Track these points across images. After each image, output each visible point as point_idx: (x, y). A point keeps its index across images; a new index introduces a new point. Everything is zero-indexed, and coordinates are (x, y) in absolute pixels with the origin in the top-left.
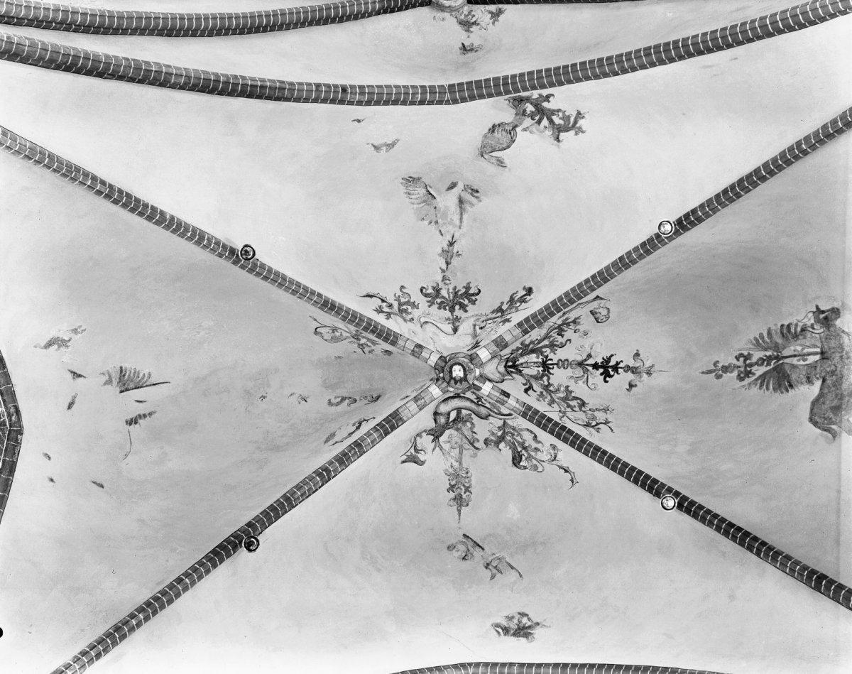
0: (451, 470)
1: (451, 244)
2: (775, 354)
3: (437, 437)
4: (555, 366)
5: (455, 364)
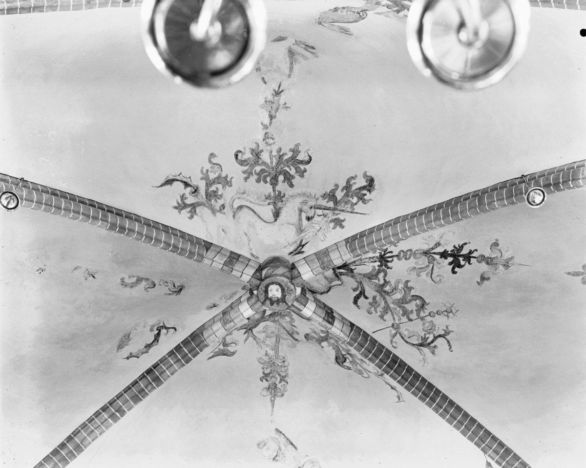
0: (266, 359)
1: (278, 93)
4: (395, 259)
5: (272, 283)
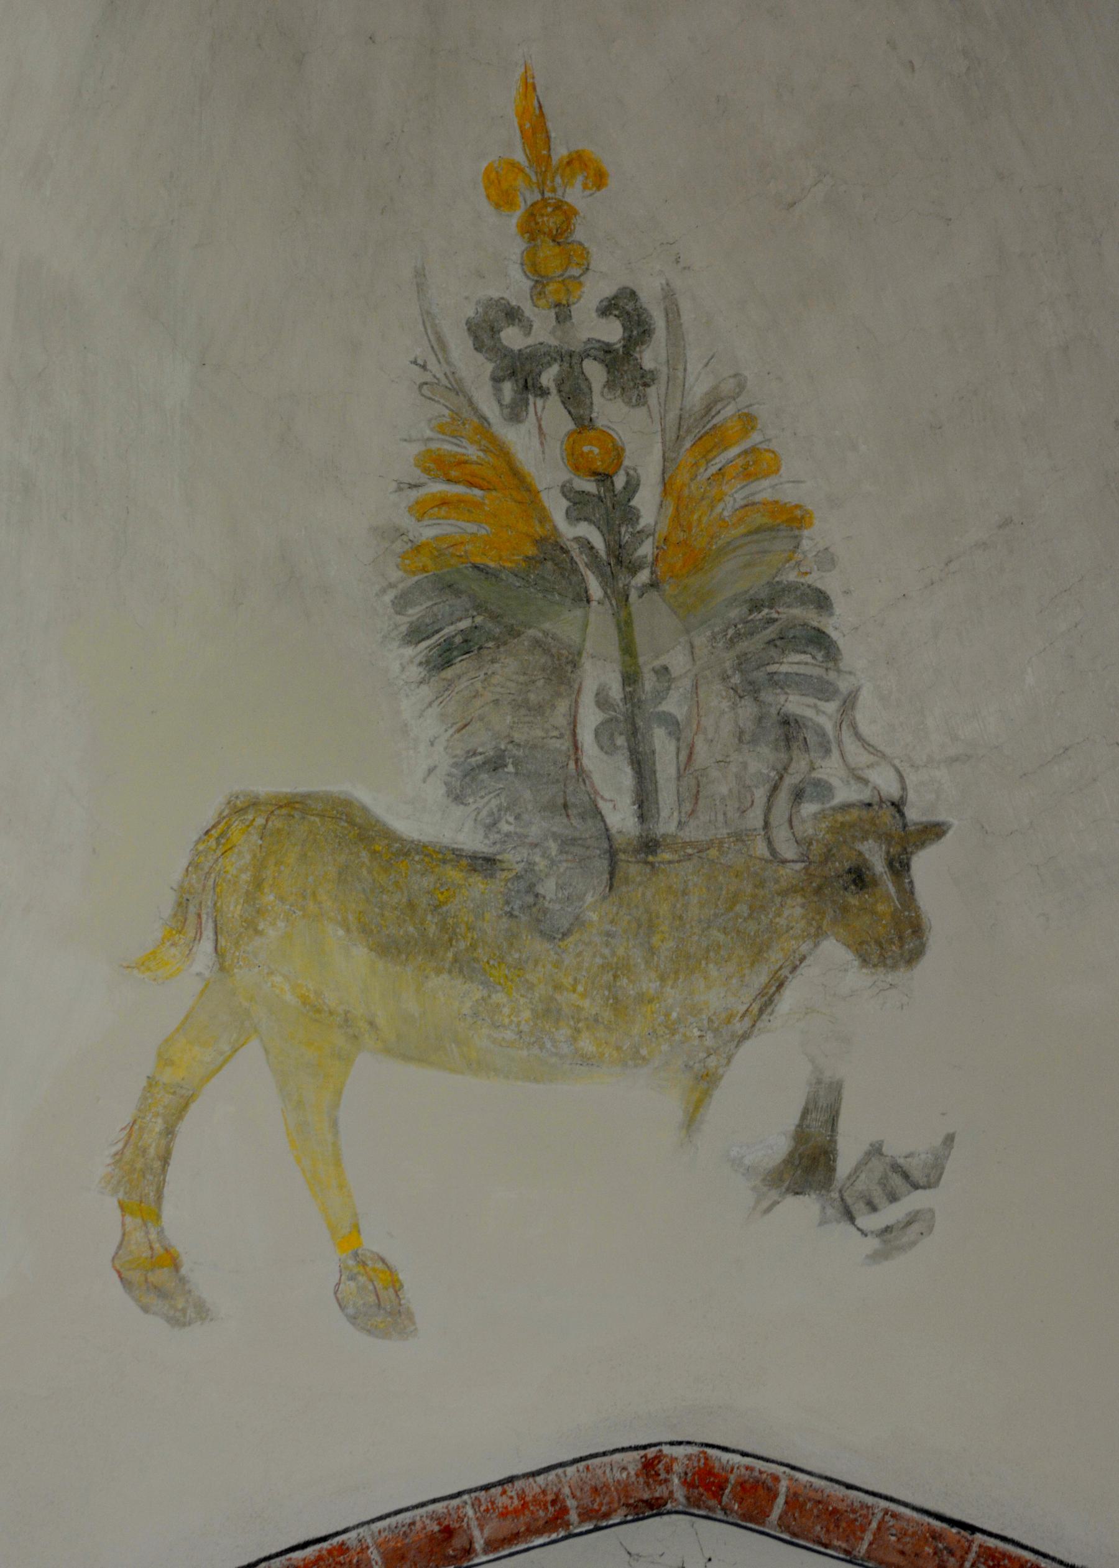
2: (646, 549)
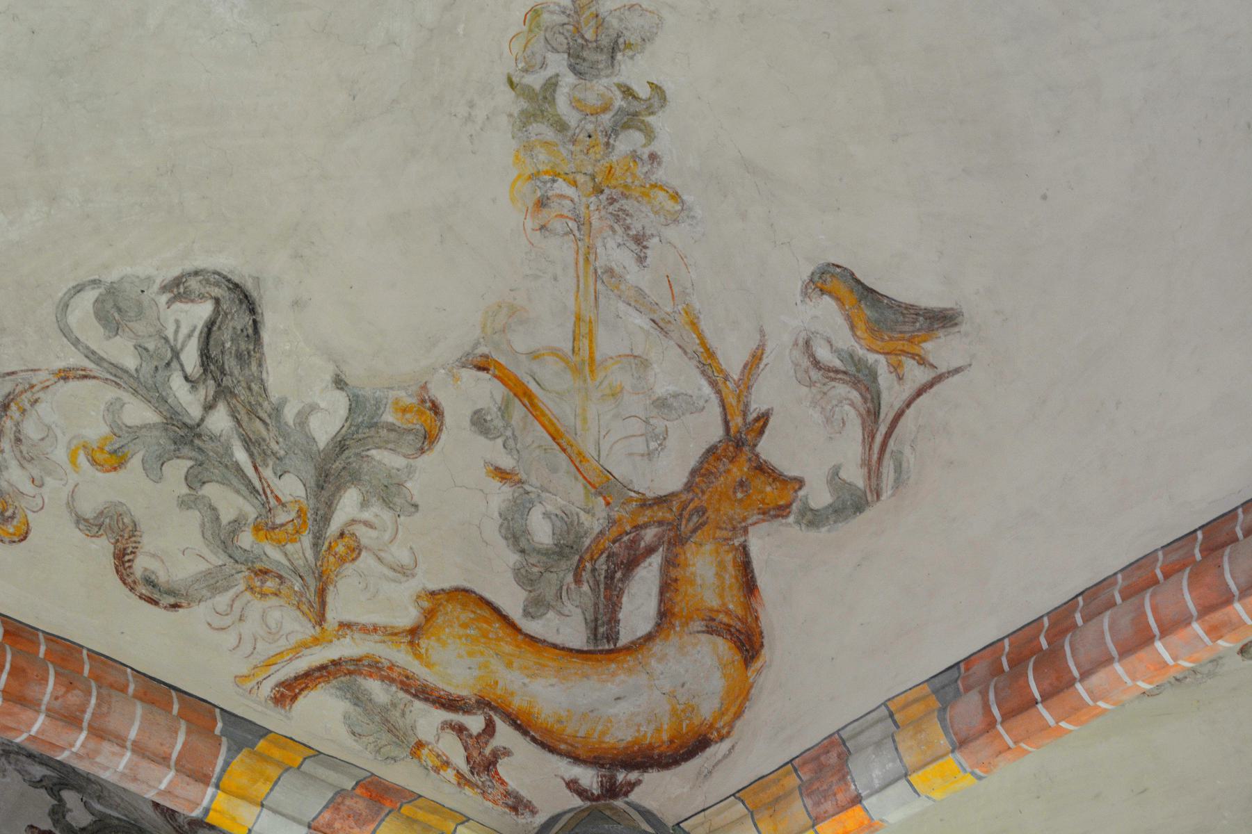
3: (739, 444)
